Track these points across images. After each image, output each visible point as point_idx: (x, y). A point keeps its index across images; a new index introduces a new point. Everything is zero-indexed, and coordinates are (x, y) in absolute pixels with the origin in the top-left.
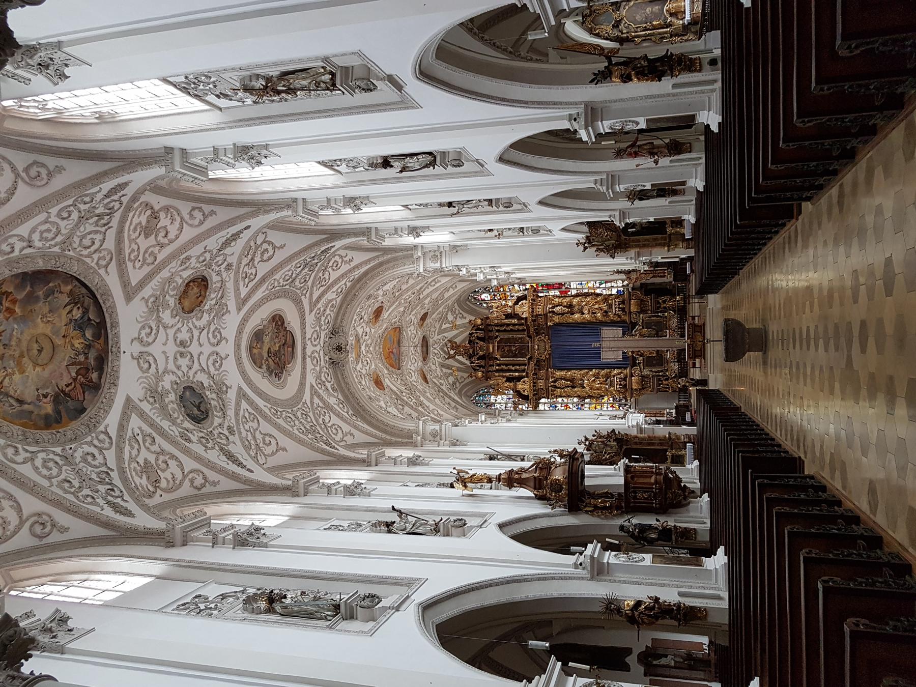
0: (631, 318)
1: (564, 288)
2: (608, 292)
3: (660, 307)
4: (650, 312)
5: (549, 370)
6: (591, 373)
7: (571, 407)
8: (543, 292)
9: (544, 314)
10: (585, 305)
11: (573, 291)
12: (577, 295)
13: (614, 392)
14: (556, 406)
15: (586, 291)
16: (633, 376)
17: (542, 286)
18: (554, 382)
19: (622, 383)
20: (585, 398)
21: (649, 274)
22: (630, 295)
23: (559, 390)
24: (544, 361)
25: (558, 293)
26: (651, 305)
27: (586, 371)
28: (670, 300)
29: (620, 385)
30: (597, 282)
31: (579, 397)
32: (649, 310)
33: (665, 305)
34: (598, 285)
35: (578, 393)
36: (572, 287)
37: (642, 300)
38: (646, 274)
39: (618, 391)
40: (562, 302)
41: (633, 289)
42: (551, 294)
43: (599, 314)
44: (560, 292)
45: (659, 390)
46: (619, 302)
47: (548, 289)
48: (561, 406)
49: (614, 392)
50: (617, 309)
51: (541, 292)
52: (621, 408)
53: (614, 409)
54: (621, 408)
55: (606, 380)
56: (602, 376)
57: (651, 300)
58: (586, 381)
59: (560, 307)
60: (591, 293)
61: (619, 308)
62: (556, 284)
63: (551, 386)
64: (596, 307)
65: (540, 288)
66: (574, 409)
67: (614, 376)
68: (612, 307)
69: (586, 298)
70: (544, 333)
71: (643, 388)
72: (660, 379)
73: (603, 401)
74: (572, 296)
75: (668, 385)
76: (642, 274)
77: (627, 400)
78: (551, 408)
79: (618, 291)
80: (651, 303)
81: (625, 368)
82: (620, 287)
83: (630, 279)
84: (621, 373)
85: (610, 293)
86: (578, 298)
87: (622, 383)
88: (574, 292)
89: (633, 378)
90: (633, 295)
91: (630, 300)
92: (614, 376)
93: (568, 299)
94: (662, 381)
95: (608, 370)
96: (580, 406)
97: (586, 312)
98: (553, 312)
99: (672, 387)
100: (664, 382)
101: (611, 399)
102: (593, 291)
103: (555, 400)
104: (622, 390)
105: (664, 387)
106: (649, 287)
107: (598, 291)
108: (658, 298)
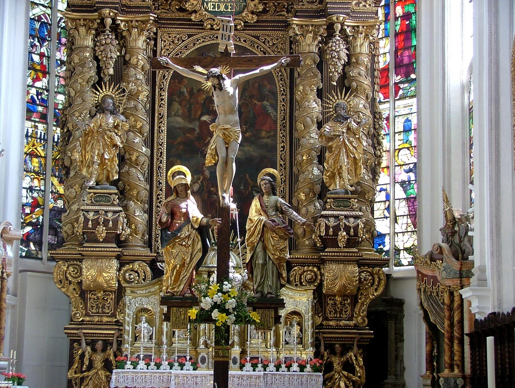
0: (303, 264)
1: (398, 79)
2: (379, 209)
3: (333, 352)
4: (319, 320)
5: (152, 17)
6: (137, 140)
7: (38, 84)
8: (387, 20)
9: (324, 10)
10: (349, 129)
11: (387, 105)
12: (376, 115)
13: (75, 207)
14: (42, 40)
15: (386, 144)
16: (122, 265)
17: (407, 16)
18: (115, 27)
19: (101, 228)
20: (62, 123)
21: (451, 318)
22: (373, 266)
23: (89, 42)
24: (182, 10)
25: (381, 66)
26: (339, 327)
27: (147, 128)
28: (354, 382)
29: (96, 223)
30: (412, 176)
31: (69, 104)
32: (326, 319)
33: (337, 366)
34: (403, 176)
35: (79, 100)
36: (397, 103)
37: (355, 300)
38: (451, 309)
39: (77, 220)
40: (357, 63)
41: (388, 276)
42: (382, 43)
43: (316, 172)
44: (386, 70)
45: (74, 341)
46: (356, 228)
47: (397, 35)
48: (42, 55)
49: (75, 207)
50: (332, 222)
51: (387, 15)
52: (29, 229)
53: (28, 211)
54: (29, 229)
55: (115, 183)
56: (128, 172)
57: (356, 327)
58: (111, 120)
59: (343, 55)
60: (380, 157)
61: (337, 229)
62: (414, 56)
63: (102, 20)
64: (344, 159)
65: (399, 11)
66: (33, 91)
67: (126, 208)
68: (338, 207)
69: (368, 135)
70: (265, 11)
71: (83, 294)
72: (111, 344)
73: (55, 181)
74: (374, 99)
75: (90, 367)
76: (451, 294)
77: (51, 247)
78: (37, 25)
79: (382, 236)
80: (346, 327)
81: (149, 244)
82: (393, 241)
83: (432, 259)
84: (135, 232)
85: (377, 214)
86: (368, 112)
87: (101, 228)
88: (385, 109)
89: (115, 263)
90: (372, 274)
91: (361, 263)
92: (126, 208)
93: (366, 82)
94: (104, 350)
95: (144, 194)
96: (40, 109)
97: (327, 128)
98: (331, 33)
99: (82, 379)
100: (98, 359)
101: (60, 204)
102: (384, 164)
103: (64, 40)
104: (79, 229)
105: (82, 356)
106: (391, 325)
107: (384, 178)
108: (359, 347)
